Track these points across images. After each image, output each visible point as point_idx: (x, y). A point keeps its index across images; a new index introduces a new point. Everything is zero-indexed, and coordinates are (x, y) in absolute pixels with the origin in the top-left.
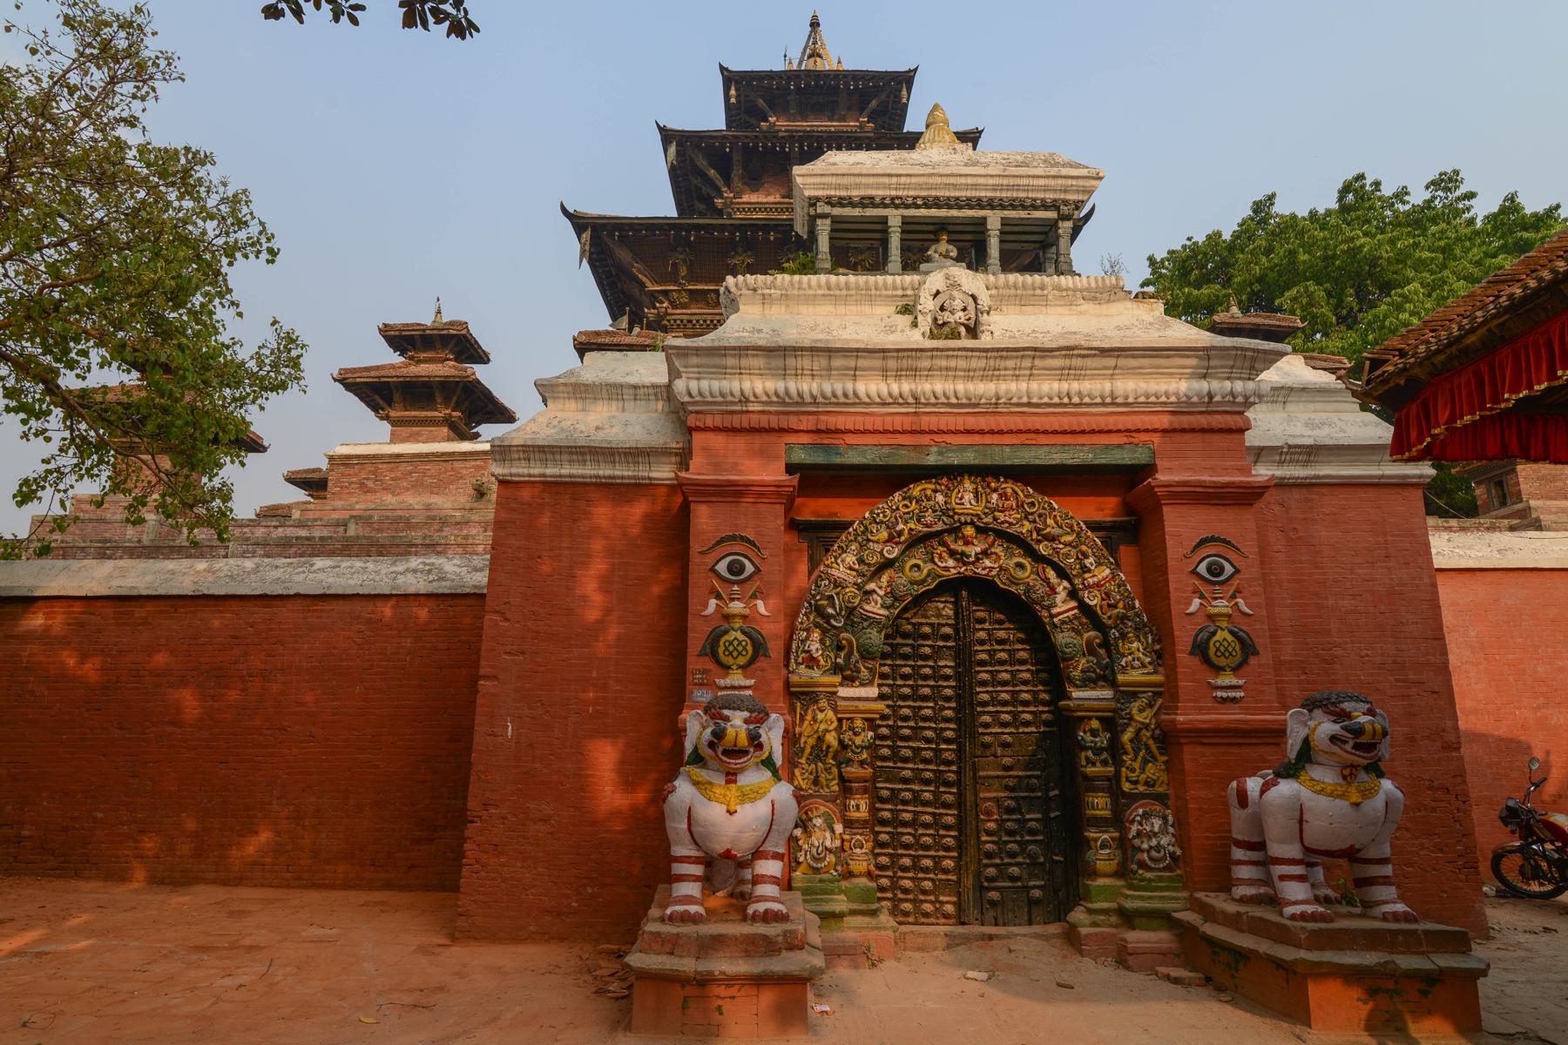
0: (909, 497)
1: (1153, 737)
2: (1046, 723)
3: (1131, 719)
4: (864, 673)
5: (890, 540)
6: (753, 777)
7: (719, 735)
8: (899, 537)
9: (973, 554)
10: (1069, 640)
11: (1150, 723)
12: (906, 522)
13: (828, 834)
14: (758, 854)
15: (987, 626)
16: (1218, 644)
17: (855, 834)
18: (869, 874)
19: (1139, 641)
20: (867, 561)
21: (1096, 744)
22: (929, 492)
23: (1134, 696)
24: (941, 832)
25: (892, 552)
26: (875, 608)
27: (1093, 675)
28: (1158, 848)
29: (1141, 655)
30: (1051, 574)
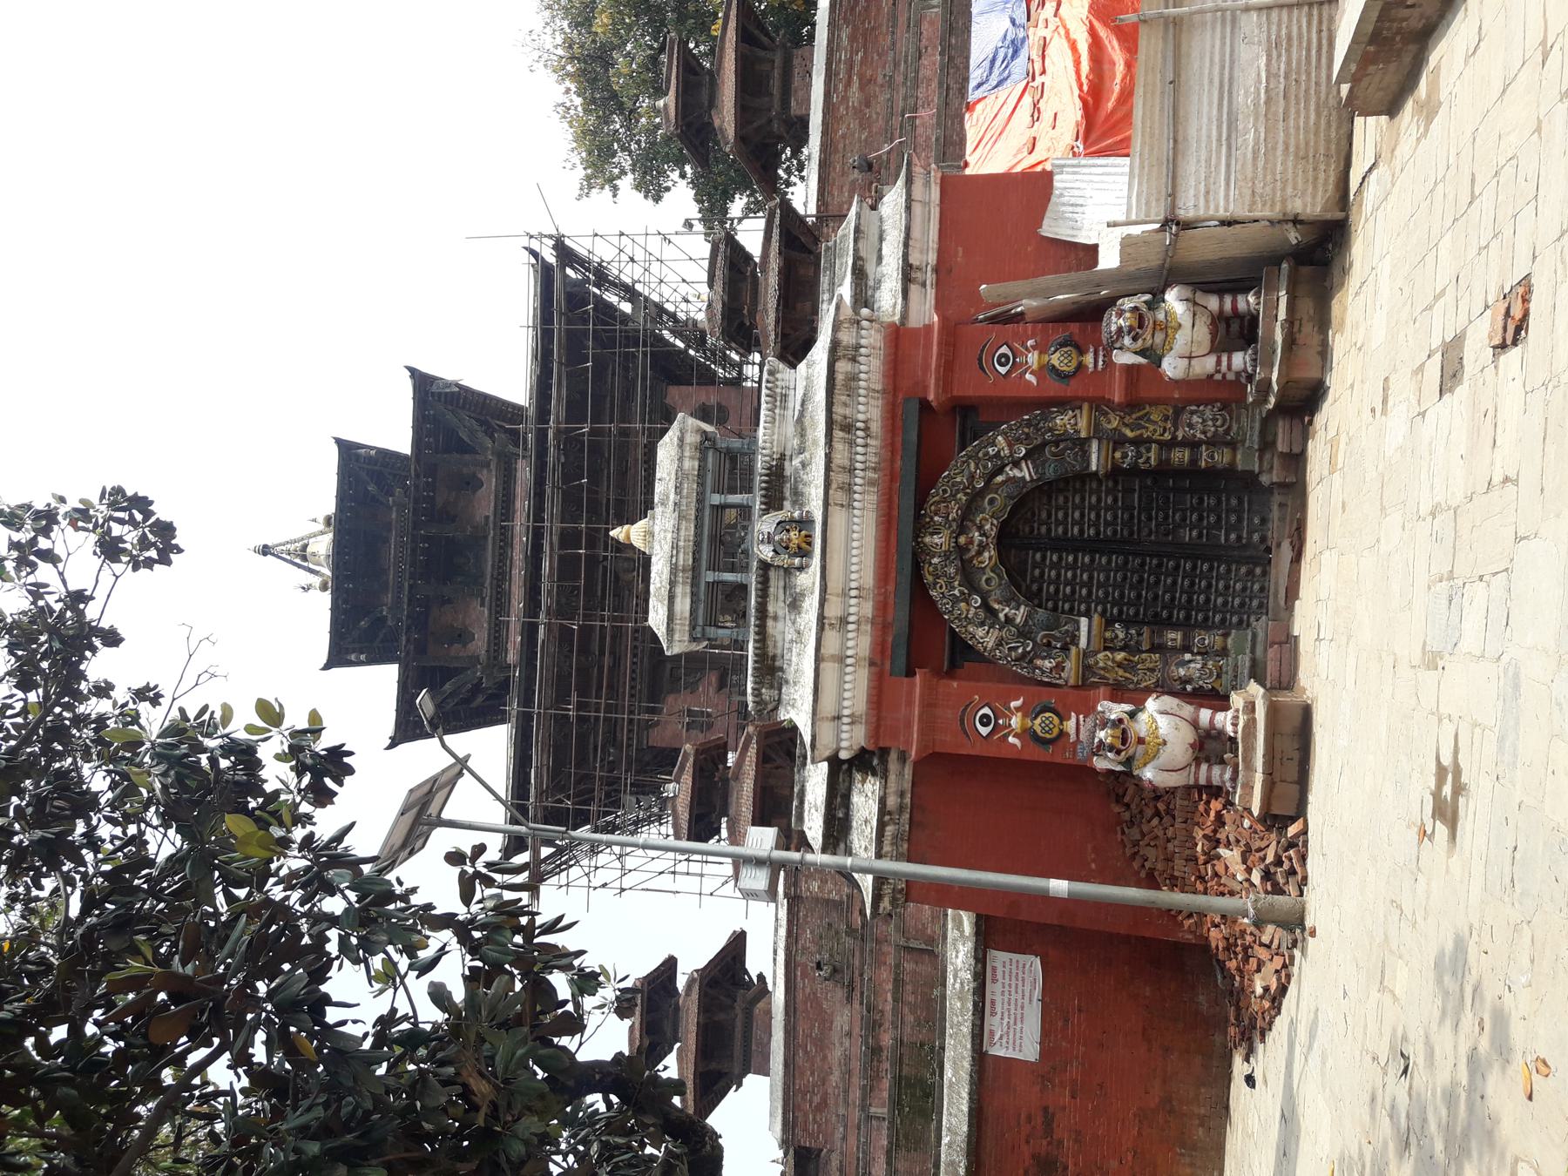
2: (1116, 482)
3: (1115, 429)
6: (1142, 725)
7: (1111, 748)
13: (1192, 665)
14: (1195, 724)
15: (1036, 525)
18: (1226, 635)
22: (931, 569)
23: (1097, 425)
26: (1020, 615)
28: (1214, 420)
30: (1000, 479)
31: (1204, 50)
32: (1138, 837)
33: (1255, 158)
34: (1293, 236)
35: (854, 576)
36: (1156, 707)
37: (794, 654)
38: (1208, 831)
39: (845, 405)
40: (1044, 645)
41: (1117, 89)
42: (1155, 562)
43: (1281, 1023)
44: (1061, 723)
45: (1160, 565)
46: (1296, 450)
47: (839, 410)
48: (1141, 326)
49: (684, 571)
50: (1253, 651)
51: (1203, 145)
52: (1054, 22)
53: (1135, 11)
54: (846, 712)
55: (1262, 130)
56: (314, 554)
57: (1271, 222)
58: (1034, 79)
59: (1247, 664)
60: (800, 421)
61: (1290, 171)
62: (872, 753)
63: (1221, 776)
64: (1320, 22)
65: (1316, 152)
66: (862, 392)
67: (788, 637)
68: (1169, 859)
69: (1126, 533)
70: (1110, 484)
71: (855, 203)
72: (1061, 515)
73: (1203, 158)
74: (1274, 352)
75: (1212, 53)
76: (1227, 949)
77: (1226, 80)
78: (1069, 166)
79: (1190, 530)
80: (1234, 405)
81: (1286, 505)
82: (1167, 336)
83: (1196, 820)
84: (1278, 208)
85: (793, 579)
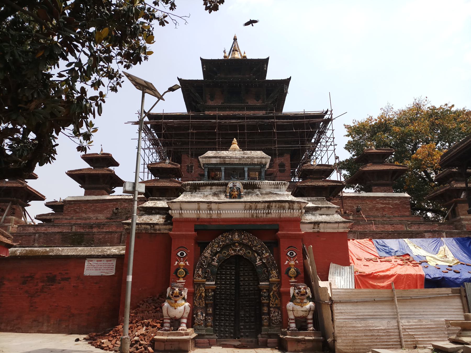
1: (277, 293)
3: (272, 289)
6: (181, 302)
7: (173, 292)
8: (220, 246)
11: (276, 291)
13: (201, 316)
14: (182, 318)
15: (243, 267)
18: (211, 326)
22: (228, 235)
23: (274, 284)
26: (215, 263)
28: (276, 319)
30: (256, 255)
31: (385, 310)
32: (149, 302)
33: (353, 327)
34: (329, 340)
35: (224, 212)
36: (186, 306)
37: (200, 195)
38: (151, 323)
39: (275, 206)
41: (376, 284)
42: (233, 303)
43: (93, 348)
44: (182, 277)
45: (232, 305)
46: (268, 345)
47: (274, 204)
48: (301, 295)
49: (224, 161)
50: (207, 335)
51: (356, 311)
52: (396, 263)
53: (396, 288)
54: (183, 212)
55: (361, 329)
56: (235, 53)
57: (334, 333)
58: (379, 259)
59: (202, 333)
60: (271, 193)
61: (349, 338)
62: (171, 220)
63: (166, 326)
64: (395, 345)
65: (356, 346)
66: (280, 211)
67: (205, 193)
68: (142, 312)
69: (242, 294)
70: (256, 289)
71: (337, 206)
72: (246, 274)
73: (352, 311)
74: (295, 336)
75: (384, 312)
76: (116, 331)
77: (376, 317)
78: (352, 270)
79: (243, 314)
80: (281, 325)
81: (252, 343)
82: (299, 303)
83: (154, 319)
84: (338, 335)
85: (223, 193)
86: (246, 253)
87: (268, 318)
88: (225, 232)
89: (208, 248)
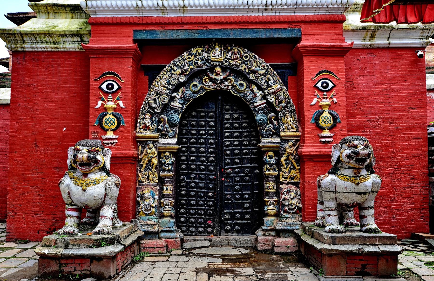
0: (191, 54)
3: (285, 151)
4: (171, 133)
5: (182, 73)
8: (186, 72)
9: (220, 79)
10: (261, 117)
11: (293, 153)
12: (189, 66)
13: (152, 200)
16: (323, 118)
17: (166, 200)
18: (171, 216)
19: (291, 117)
20: (171, 83)
21: (270, 162)
22: (200, 51)
23: (288, 141)
24: (208, 199)
25: (183, 79)
26: (176, 104)
27: (271, 133)
29: (292, 124)
30: (255, 88)
40: (159, 119)
44: (112, 130)
70: (255, 151)
72: (236, 125)
86: (235, 86)
87: (275, 201)
88: (195, 47)
89: (163, 77)
